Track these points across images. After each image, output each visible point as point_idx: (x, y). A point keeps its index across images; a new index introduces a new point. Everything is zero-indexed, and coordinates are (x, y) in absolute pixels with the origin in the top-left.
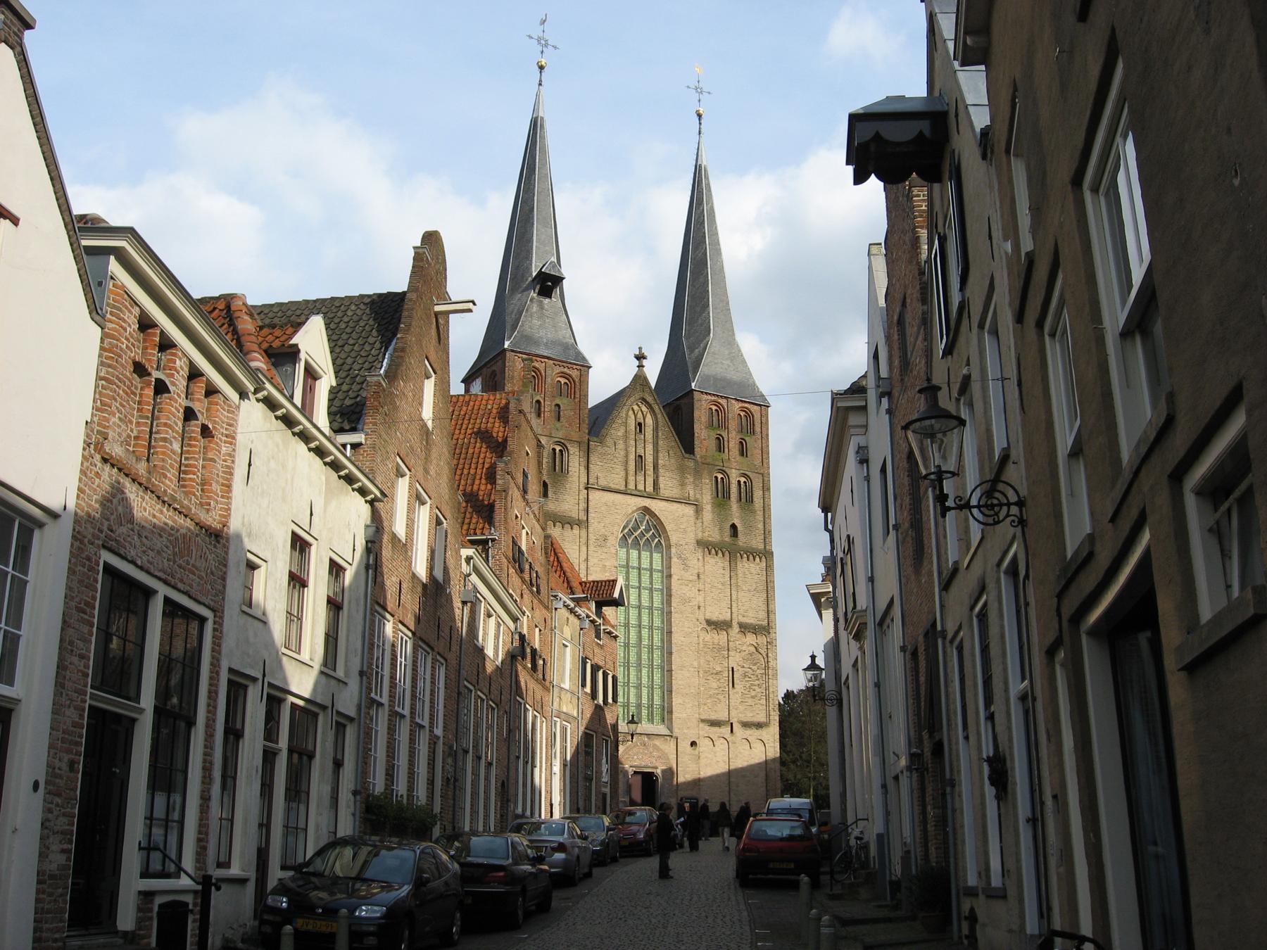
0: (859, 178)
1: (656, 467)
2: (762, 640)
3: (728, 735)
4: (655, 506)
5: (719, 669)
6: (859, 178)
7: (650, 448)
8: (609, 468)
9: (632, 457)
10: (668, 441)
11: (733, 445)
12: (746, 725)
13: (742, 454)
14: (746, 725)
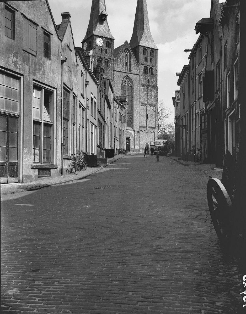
0: (197, 33)
1: (130, 65)
2: (154, 108)
3: (146, 130)
4: (129, 75)
5: (144, 114)
6: (197, 33)
8: (119, 66)
9: (124, 63)
10: (133, 59)
11: (149, 61)
13: (151, 62)
14: (150, 127)
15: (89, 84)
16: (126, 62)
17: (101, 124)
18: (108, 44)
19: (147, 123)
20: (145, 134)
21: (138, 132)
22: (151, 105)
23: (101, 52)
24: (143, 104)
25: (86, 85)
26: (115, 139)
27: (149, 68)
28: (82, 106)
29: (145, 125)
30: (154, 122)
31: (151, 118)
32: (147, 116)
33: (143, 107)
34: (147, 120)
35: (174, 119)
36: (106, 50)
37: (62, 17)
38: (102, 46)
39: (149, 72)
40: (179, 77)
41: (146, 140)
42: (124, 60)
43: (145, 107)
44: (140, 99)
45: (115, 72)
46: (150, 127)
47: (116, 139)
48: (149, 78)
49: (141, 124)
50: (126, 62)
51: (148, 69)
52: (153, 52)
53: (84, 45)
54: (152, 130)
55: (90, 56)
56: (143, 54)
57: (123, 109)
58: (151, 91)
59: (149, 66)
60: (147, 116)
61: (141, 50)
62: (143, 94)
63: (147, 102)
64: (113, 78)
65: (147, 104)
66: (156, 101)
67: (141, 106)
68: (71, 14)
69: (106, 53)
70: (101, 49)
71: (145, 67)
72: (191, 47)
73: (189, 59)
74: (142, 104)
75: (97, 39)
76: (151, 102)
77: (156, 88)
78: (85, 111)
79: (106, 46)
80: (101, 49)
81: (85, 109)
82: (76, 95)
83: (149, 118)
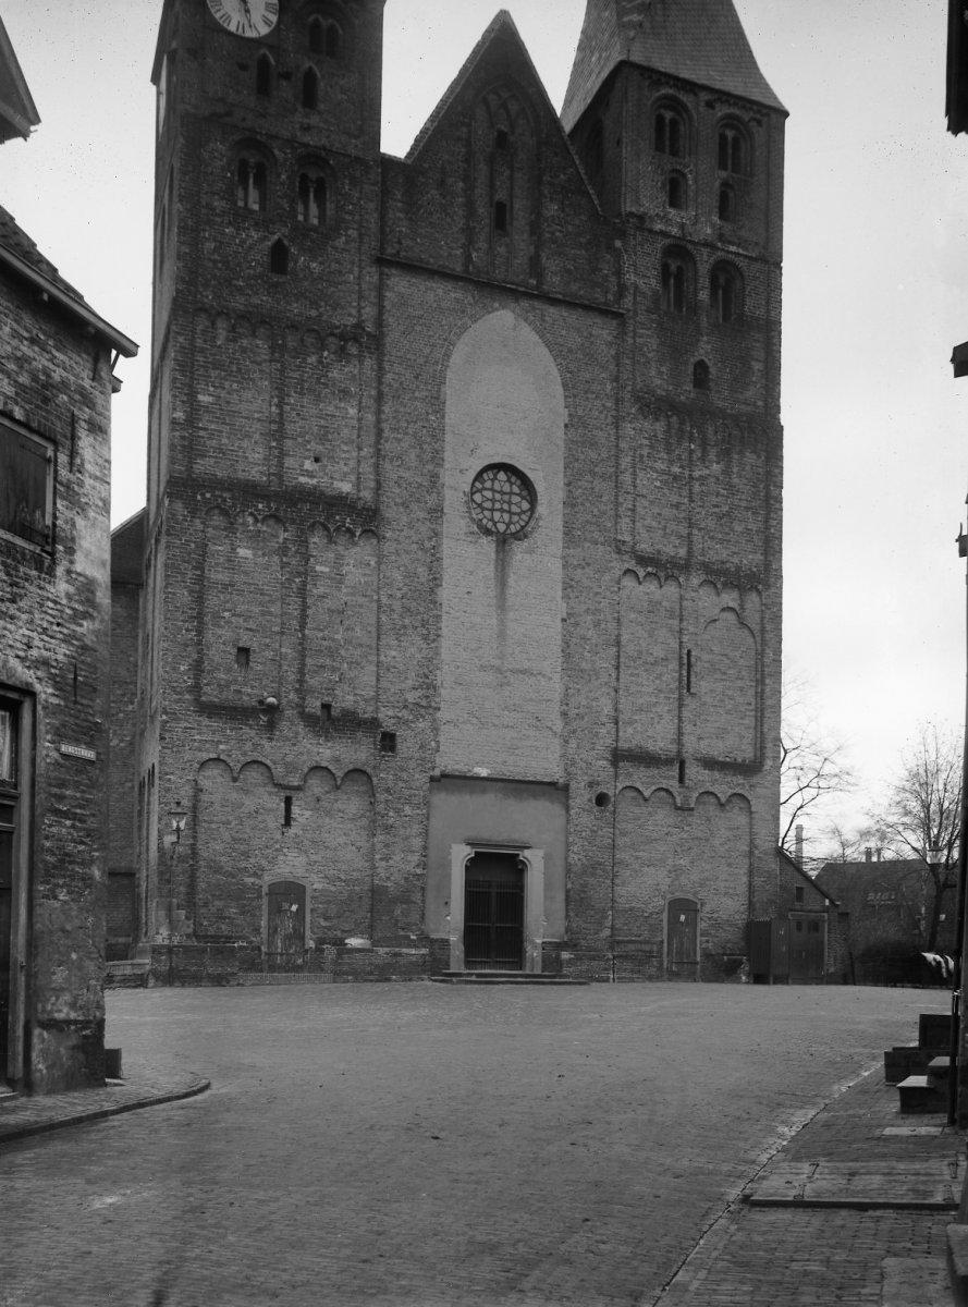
3: (674, 785)
5: (658, 652)
19: (687, 728)
21: (601, 800)
22: (721, 577)
23: (263, 88)
24: (658, 567)
27: (705, 262)
30: (750, 721)
31: (719, 686)
32: (687, 663)
33: (651, 586)
34: (688, 700)
36: (310, 78)
38: (271, 42)
39: (704, 295)
41: (676, 871)
43: (671, 589)
44: (625, 523)
45: (399, 284)
46: (710, 763)
48: (705, 349)
49: (631, 738)
50: (501, 196)
54: (723, 786)
56: (659, 147)
59: (705, 251)
60: (687, 663)
62: (647, 481)
63: (682, 552)
65: (686, 567)
67: (628, 582)
70: (263, 62)
74: (643, 560)
76: (718, 553)
83: (702, 686)
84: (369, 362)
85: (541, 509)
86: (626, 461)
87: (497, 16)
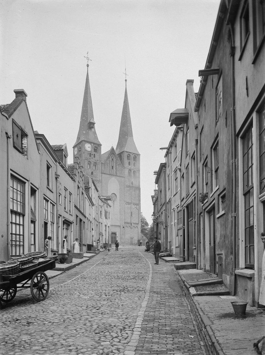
0: (171, 125)
1: (116, 169)
2: (138, 206)
5: (129, 212)
6: (171, 125)
7: (115, 163)
12: (134, 223)
14: (134, 223)
15: (59, 177)
16: (112, 166)
17: (81, 220)
18: (96, 149)
20: (130, 229)
21: (123, 227)
22: (135, 204)
23: (90, 156)
24: (129, 203)
25: (56, 178)
26: (100, 234)
28: (50, 201)
29: (129, 221)
35: (152, 215)
36: (94, 154)
37: (15, 94)
38: (91, 151)
40: (156, 175)
42: (111, 164)
43: (130, 205)
44: (125, 199)
45: (103, 175)
47: (101, 234)
50: (113, 165)
51: (132, 172)
52: (136, 157)
53: (75, 150)
55: (63, 149)
56: (128, 159)
57: (108, 206)
58: (135, 191)
61: (125, 155)
64: (101, 180)
66: (139, 200)
67: (126, 205)
68: (26, 92)
69: (94, 157)
70: (90, 153)
71: (129, 170)
72: (167, 145)
73: (165, 157)
74: (127, 203)
75: (86, 144)
77: (139, 189)
78: (55, 207)
79: (95, 151)
80: (90, 153)
81: (56, 204)
82: (38, 188)
84: (101, 184)
85: (117, 198)
86: (125, 193)
87: (112, 147)
